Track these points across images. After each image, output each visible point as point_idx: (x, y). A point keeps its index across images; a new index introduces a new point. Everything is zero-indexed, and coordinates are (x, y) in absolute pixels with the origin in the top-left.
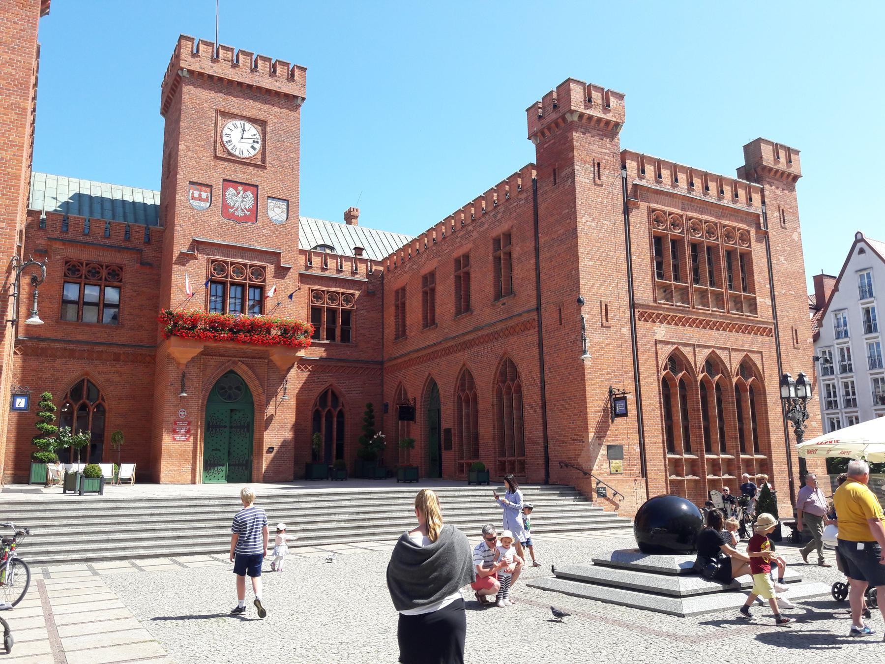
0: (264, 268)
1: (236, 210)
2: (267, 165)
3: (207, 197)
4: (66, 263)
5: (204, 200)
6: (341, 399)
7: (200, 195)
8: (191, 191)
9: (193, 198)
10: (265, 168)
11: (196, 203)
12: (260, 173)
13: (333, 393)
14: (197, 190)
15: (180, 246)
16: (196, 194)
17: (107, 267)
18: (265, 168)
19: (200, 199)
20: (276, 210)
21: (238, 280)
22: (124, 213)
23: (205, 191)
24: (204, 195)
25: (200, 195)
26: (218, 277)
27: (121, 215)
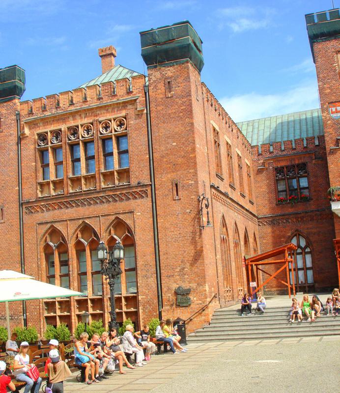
4: (276, 169)
7: (336, 109)
8: (330, 109)
11: (334, 115)
14: (334, 107)
15: (330, 145)
16: (334, 109)
17: (297, 166)
22: (307, 128)
25: (336, 109)
27: (305, 130)
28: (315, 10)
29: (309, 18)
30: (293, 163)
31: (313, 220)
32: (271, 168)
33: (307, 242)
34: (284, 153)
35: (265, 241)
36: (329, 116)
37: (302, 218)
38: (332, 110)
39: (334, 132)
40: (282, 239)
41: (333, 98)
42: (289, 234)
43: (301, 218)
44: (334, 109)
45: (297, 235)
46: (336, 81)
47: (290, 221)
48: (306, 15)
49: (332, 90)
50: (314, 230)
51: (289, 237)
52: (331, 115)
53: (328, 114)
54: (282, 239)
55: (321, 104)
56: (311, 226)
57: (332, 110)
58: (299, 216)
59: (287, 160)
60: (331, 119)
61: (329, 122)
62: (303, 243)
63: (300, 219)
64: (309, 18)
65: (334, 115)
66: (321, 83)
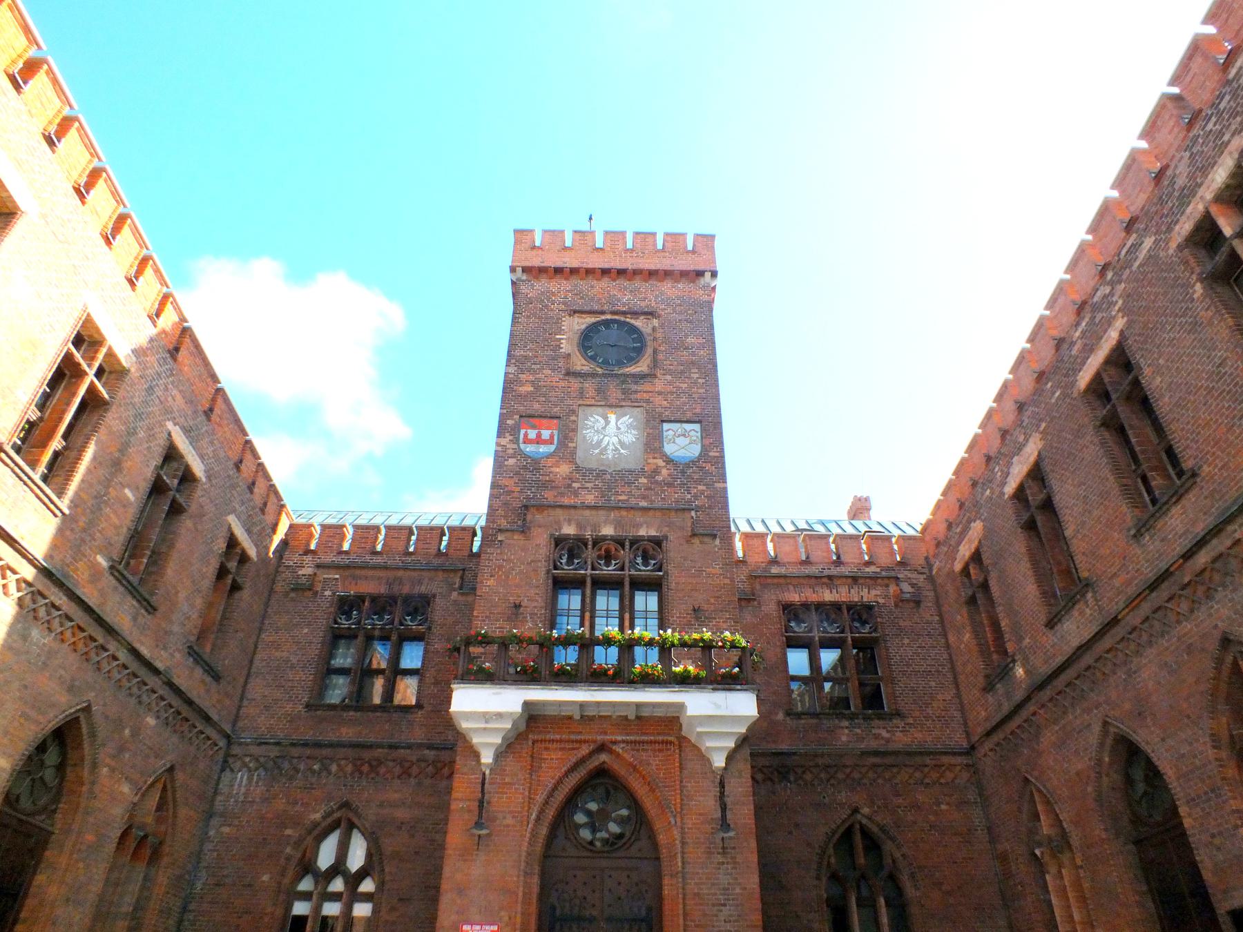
0: (657, 542)
1: (605, 449)
2: (659, 372)
3: (552, 436)
5: (545, 442)
6: (888, 847)
7: (539, 435)
8: (523, 432)
9: (527, 441)
10: (655, 376)
12: (647, 387)
13: (865, 833)
14: (533, 428)
16: (532, 434)
18: (655, 376)
19: (539, 441)
20: (681, 441)
21: (609, 570)
23: (548, 428)
24: (546, 434)
25: (539, 435)
26: (567, 570)
28: (538, 226)
29: (521, 236)
30: (396, 589)
31: (410, 776)
32: (327, 593)
33: (369, 856)
34: (378, 560)
35: (226, 830)
36: (515, 446)
37: (375, 765)
38: (526, 435)
39: (518, 489)
40: (288, 832)
41: (536, 406)
42: (317, 816)
43: (369, 763)
44: (532, 434)
45: (343, 824)
46: (553, 370)
47: (334, 768)
48: (516, 232)
49: (537, 388)
50: (401, 814)
51: (316, 825)
52: (522, 446)
53: (516, 441)
54: (288, 832)
55: (501, 415)
56: (397, 796)
57: (526, 435)
58: (367, 755)
59: (380, 578)
60: (519, 453)
61: (511, 461)
62: (357, 858)
63: (366, 768)
64: (521, 236)
65: (529, 449)
66: (512, 369)
